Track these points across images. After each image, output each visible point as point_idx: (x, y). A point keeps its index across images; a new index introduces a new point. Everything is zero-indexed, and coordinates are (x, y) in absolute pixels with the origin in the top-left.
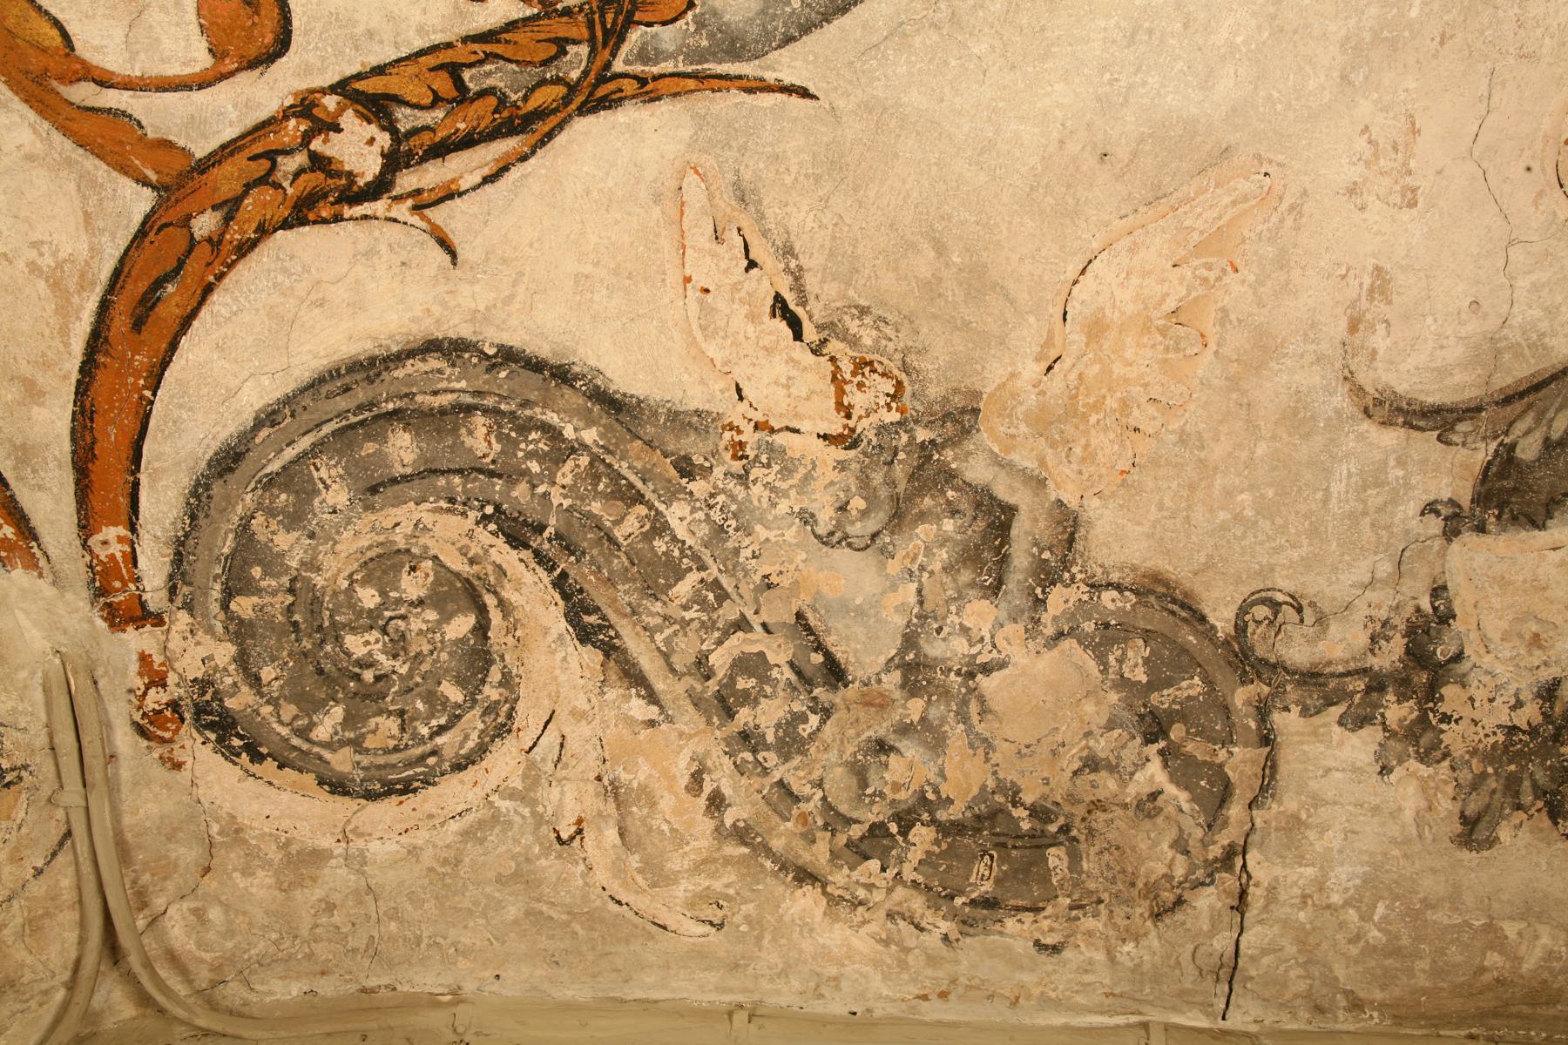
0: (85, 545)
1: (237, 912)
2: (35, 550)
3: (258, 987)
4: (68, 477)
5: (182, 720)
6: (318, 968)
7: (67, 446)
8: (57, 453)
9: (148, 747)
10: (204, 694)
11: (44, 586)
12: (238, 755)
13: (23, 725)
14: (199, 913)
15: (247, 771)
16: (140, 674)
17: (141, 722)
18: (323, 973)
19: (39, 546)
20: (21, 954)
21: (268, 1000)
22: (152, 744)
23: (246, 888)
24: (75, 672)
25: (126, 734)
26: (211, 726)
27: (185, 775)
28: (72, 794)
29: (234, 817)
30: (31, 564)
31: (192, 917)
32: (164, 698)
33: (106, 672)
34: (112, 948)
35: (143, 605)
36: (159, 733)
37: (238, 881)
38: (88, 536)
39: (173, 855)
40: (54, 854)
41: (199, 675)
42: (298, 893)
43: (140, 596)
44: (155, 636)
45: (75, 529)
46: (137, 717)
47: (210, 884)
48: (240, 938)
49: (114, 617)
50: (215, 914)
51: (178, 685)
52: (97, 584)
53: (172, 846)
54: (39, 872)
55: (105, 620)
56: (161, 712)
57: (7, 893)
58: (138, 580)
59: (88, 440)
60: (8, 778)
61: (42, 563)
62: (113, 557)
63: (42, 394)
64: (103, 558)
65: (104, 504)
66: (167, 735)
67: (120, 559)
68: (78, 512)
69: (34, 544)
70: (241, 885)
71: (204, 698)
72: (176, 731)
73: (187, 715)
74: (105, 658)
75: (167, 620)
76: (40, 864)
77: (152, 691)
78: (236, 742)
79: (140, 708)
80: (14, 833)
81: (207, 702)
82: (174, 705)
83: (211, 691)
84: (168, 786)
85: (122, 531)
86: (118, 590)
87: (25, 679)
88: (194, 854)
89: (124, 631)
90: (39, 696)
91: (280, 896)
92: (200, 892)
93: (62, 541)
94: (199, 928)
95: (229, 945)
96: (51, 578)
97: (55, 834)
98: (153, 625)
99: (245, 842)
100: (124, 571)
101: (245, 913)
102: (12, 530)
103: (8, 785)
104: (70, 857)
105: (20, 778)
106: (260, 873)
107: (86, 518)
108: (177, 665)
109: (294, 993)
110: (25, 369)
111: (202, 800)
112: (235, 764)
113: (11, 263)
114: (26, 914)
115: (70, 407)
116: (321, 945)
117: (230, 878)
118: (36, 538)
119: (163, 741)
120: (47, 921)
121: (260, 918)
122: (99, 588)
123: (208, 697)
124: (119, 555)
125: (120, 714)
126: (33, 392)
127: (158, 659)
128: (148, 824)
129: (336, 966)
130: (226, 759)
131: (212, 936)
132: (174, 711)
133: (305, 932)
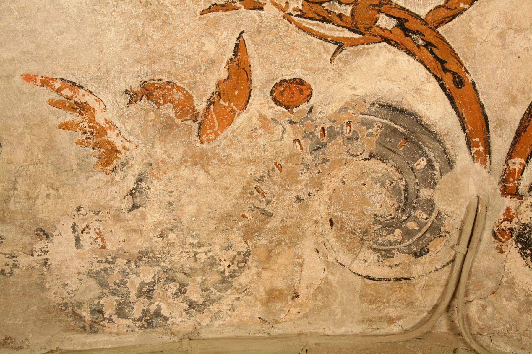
0: (506, 162)
1: (498, 312)
2: (488, 158)
3: (494, 342)
4: (512, 135)
5: (512, 236)
6: (521, 346)
7: (517, 124)
8: (512, 126)
9: (494, 241)
10: (524, 230)
11: (485, 172)
12: (527, 257)
13: (454, 218)
14: (484, 307)
15: (527, 264)
16: (504, 215)
17: (496, 232)
18: (522, 348)
19: (490, 157)
20: (418, 295)
21: (497, 348)
22: (496, 241)
23: (505, 305)
24: (482, 206)
25: (488, 234)
26: (521, 243)
27: (504, 256)
28: (462, 249)
29: (514, 278)
30: (484, 163)
31: (481, 307)
32: (509, 226)
33: (492, 210)
34: (449, 307)
35: (517, 190)
36: (501, 238)
37: (504, 301)
38: (509, 159)
39: (485, 283)
40: (444, 266)
41: (526, 223)
42: (525, 315)
43: (518, 186)
44: (516, 203)
45: (506, 155)
46: (495, 229)
47: (492, 298)
48: (495, 322)
49: (505, 191)
50: (489, 309)
51: (516, 223)
52: (504, 177)
53: (486, 279)
54: (437, 270)
55: (501, 191)
56: (505, 230)
57: (423, 273)
58: (520, 180)
59: (526, 124)
60: (441, 234)
61: (488, 163)
62: (515, 169)
63: (517, 102)
64: (511, 168)
65: (521, 149)
66: (503, 240)
67: (517, 171)
68: (510, 149)
69: (488, 156)
70: (504, 303)
71: (524, 232)
72: (507, 240)
73: (514, 235)
74: (494, 204)
75: (524, 198)
76: (438, 268)
77: (505, 222)
78: (529, 252)
79: (498, 226)
80: (435, 254)
81: (525, 233)
82: (511, 230)
83: (528, 230)
84: (495, 258)
85: (523, 161)
86: (510, 182)
87: (462, 202)
88: (492, 285)
89: (506, 197)
90: (464, 210)
91: (517, 313)
92: (488, 299)
93: (499, 158)
94: (481, 312)
95: (490, 322)
96: (488, 170)
97: (449, 258)
98: (517, 199)
99: (513, 288)
100: (516, 176)
101: (501, 314)
102: (483, 149)
103: (440, 237)
104: (450, 269)
105: (445, 236)
106: (513, 302)
107: (512, 152)
108: (519, 216)
109: (508, 351)
110: (515, 92)
111: (505, 267)
112: (524, 259)
113: (528, 51)
114: (426, 282)
115: (525, 110)
116: (526, 338)
117: (501, 299)
118: (490, 154)
119: (501, 241)
120: (432, 288)
121: (506, 318)
122: (504, 179)
123: (526, 232)
124: (517, 169)
125: (490, 226)
126: (514, 101)
127: (513, 211)
128: (482, 268)
129: (529, 348)
130: (522, 256)
131: (485, 316)
132: (510, 232)
133: (521, 330)
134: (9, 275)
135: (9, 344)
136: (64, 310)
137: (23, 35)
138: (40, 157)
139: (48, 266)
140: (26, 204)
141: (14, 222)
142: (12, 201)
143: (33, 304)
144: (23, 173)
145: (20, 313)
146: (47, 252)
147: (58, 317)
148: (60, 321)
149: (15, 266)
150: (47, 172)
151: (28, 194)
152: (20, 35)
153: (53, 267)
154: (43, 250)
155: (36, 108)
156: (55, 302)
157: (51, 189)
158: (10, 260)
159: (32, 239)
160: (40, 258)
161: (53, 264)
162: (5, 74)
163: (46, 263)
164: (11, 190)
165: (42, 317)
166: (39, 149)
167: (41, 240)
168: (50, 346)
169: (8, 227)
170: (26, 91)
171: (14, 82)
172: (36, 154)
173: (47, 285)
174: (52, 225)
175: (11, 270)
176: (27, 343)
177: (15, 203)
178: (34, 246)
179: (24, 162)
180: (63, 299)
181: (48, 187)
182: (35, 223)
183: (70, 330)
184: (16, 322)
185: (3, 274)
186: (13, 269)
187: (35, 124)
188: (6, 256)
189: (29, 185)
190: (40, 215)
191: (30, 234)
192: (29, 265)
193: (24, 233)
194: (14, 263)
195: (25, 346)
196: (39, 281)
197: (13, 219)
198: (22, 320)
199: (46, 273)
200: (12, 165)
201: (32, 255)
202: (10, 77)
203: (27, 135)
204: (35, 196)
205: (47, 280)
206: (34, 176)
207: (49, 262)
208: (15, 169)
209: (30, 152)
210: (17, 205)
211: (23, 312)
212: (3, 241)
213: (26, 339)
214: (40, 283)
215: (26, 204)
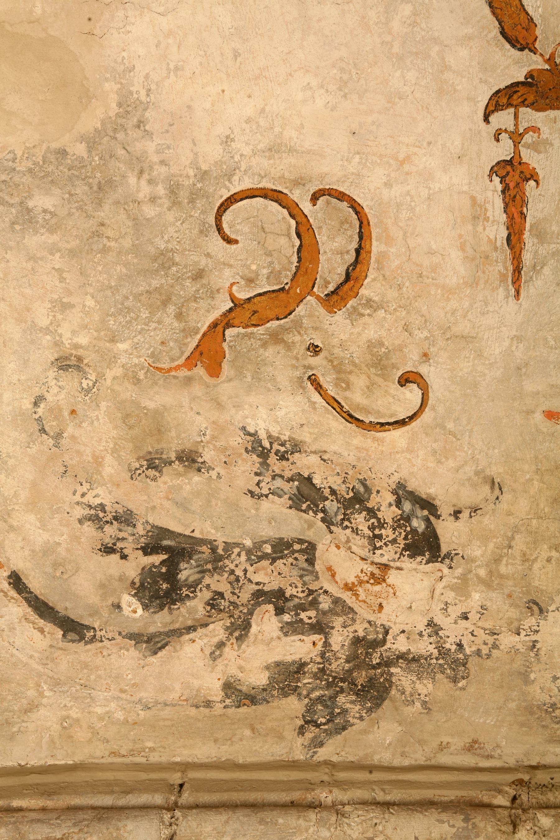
134: (486, 657)
135: (476, 749)
136: (550, 713)
137: (555, 366)
138: (546, 510)
139: (537, 651)
140: (520, 568)
141: (503, 589)
142: (504, 561)
143: (511, 699)
144: (523, 529)
145: (493, 709)
146: (537, 631)
147: (541, 721)
148: (543, 726)
149: (495, 646)
150: (552, 529)
151: (524, 555)
152: (552, 366)
153: (542, 653)
154: (533, 628)
155: (552, 451)
156: (539, 700)
157: (554, 551)
158: (489, 637)
159: (521, 613)
160: (527, 638)
161: (544, 649)
162: (524, 409)
163: (534, 646)
164: (505, 547)
165: (521, 719)
166: (547, 500)
167: (532, 615)
168: (529, 760)
169: (494, 595)
170: (545, 430)
171: (533, 418)
172: (542, 506)
173: (532, 676)
174: (548, 597)
175: (490, 651)
176: (499, 751)
177: (507, 565)
178: (522, 622)
179: (527, 515)
180: (551, 697)
181: (550, 548)
182: (528, 593)
183: (556, 740)
184: (488, 722)
185: (479, 656)
186: (492, 650)
187: (547, 470)
188: (487, 632)
189: (528, 543)
190: (536, 583)
191: (519, 607)
192: (513, 647)
193: (511, 605)
194: (494, 643)
195: (496, 756)
196: (522, 669)
197: (502, 585)
198: (495, 720)
199: (533, 660)
200: (511, 517)
201: (519, 634)
202: (529, 412)
203: (535, 482)
204: (533, 557)
205: (533, 669)
206: (536, 533)
207: (538, 646)
208: (514, 523)
209: (536, 503)
210: (510, 567)
211: (497, 708)
212: (485, 612)
213: (498, 746)
214: (524, 672)
215: (521, 567)
